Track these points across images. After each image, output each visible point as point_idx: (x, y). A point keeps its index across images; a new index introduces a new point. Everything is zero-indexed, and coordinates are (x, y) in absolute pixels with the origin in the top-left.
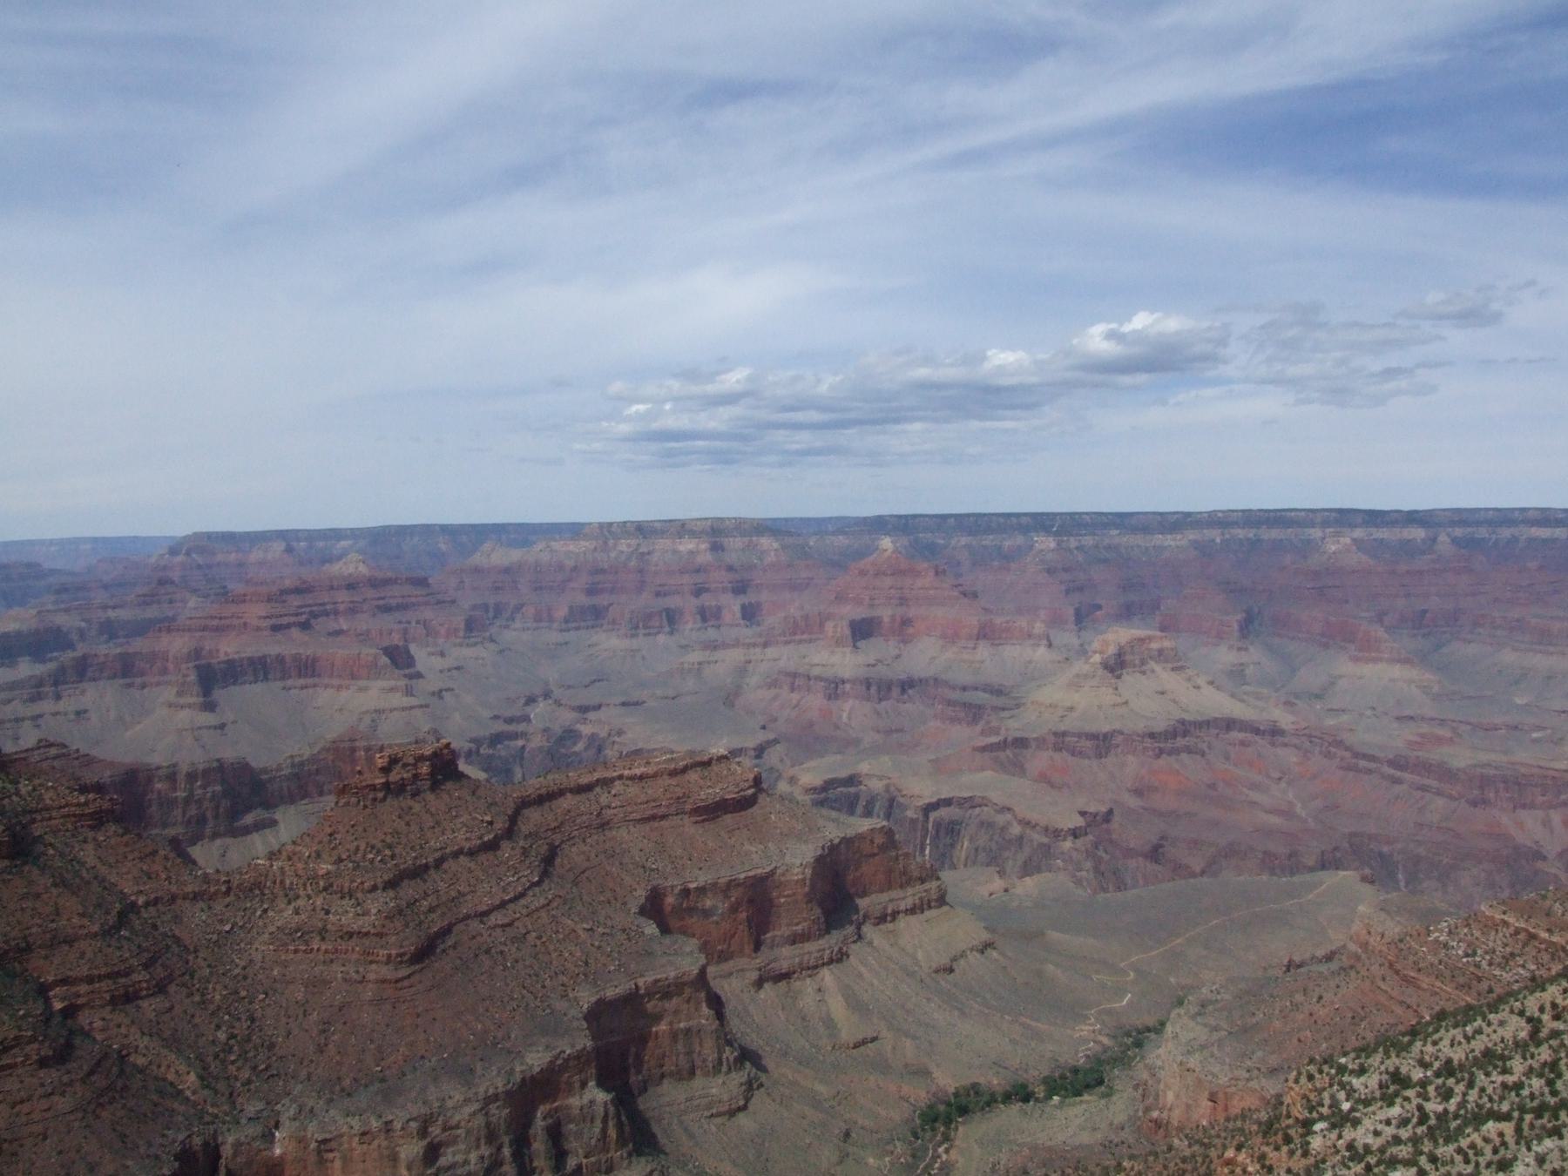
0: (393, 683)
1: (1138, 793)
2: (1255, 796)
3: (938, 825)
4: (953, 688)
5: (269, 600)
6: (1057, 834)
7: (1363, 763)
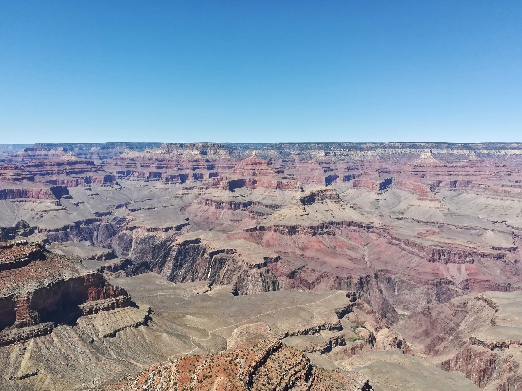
0: (52, 200)
1: (302, 249)
2: (348, 252)
3: (216, 260)
4: (263, 205)
5: (15, 169)
6: (250, 266)
7: (395, 241)
